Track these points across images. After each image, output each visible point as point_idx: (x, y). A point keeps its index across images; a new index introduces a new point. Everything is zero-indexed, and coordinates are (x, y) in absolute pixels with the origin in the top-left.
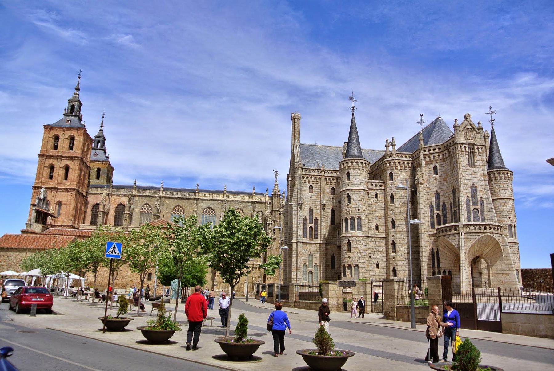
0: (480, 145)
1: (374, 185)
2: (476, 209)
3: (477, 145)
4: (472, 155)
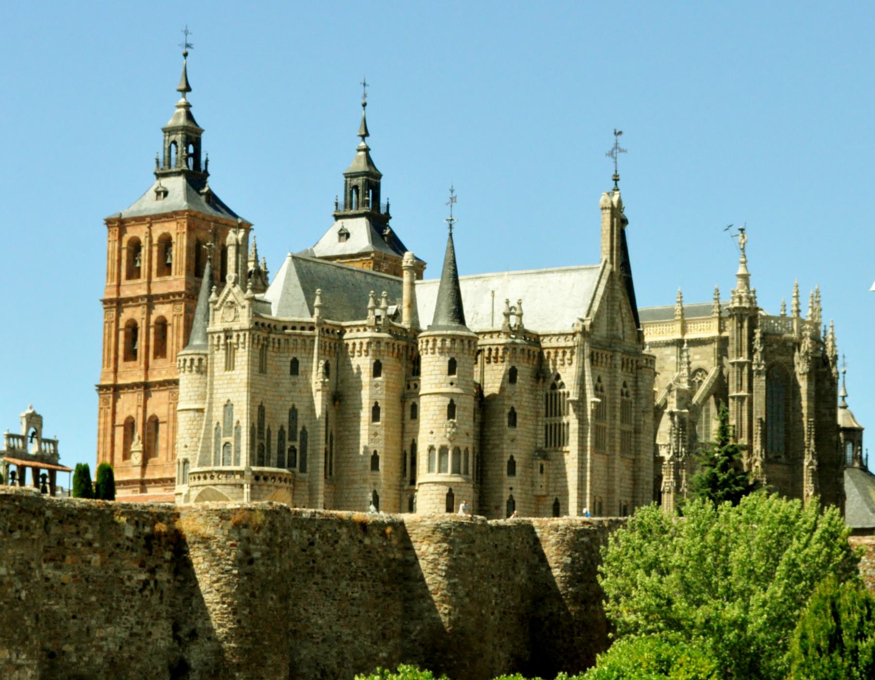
0: (241, 330)
3: (237, 331)
4: (230, 350)
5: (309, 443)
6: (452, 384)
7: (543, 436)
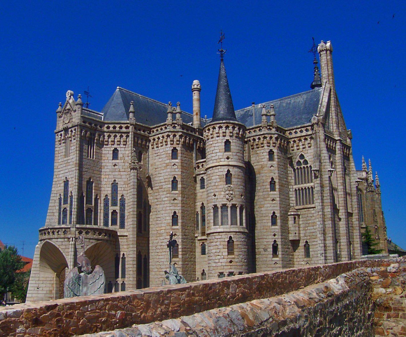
2: (65, 208)
5: (126, 208)
6: (228, 158)
7: (294, 199)
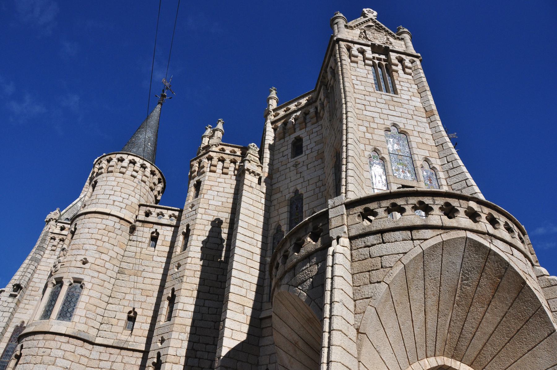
1: (154, 214)
